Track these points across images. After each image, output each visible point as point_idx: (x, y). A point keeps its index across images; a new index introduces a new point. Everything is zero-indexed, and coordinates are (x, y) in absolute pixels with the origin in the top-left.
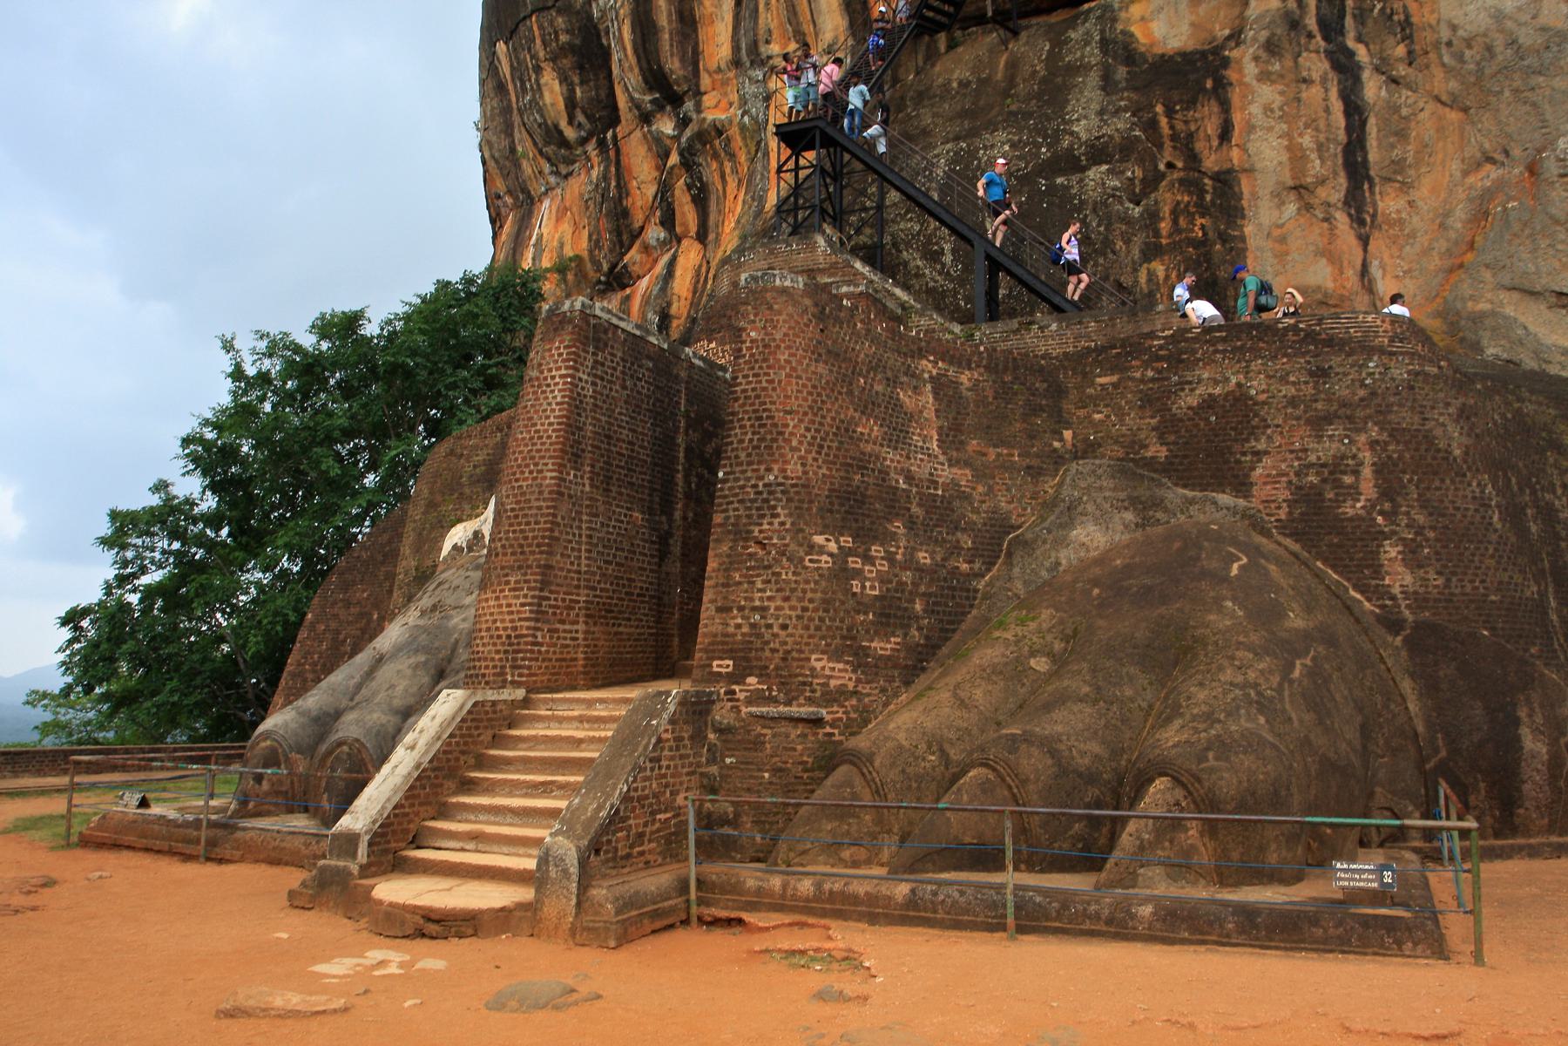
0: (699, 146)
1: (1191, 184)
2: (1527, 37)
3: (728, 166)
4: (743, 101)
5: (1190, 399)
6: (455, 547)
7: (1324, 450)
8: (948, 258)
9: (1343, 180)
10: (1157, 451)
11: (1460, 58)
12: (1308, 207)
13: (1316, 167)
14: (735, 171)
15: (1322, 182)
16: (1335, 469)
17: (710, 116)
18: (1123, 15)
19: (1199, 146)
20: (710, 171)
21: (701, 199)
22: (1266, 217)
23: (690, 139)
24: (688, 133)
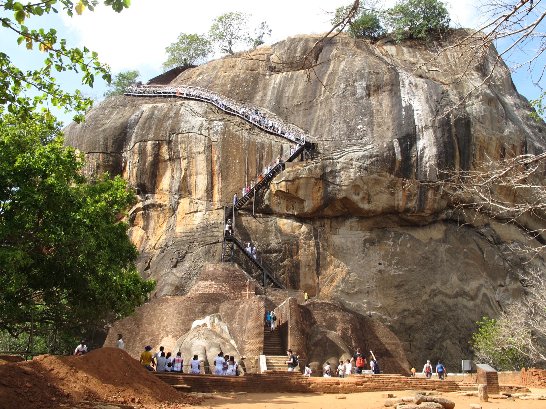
0: (151, 206)
1: (291, 262)
2: (345, 247)
3: (161, 215)
4: (170, 201)
5: (328, 317)
6: (198, 325)
7: (345, 327)
8: (243, 265)
9: (316, 265)
10: (324, 324)
11: (335, 248)
12: (310, 269)
13: (312, 263)
14: (163, 217)
15: (312, 265)
16: (346, 329)
17: (159, 202)
18: (278, 223)
19: (293, 254)
20: (153, 213)
21: (147, 218)
22: (303, 270)
23: (150, 204)
24: (148, 202)
